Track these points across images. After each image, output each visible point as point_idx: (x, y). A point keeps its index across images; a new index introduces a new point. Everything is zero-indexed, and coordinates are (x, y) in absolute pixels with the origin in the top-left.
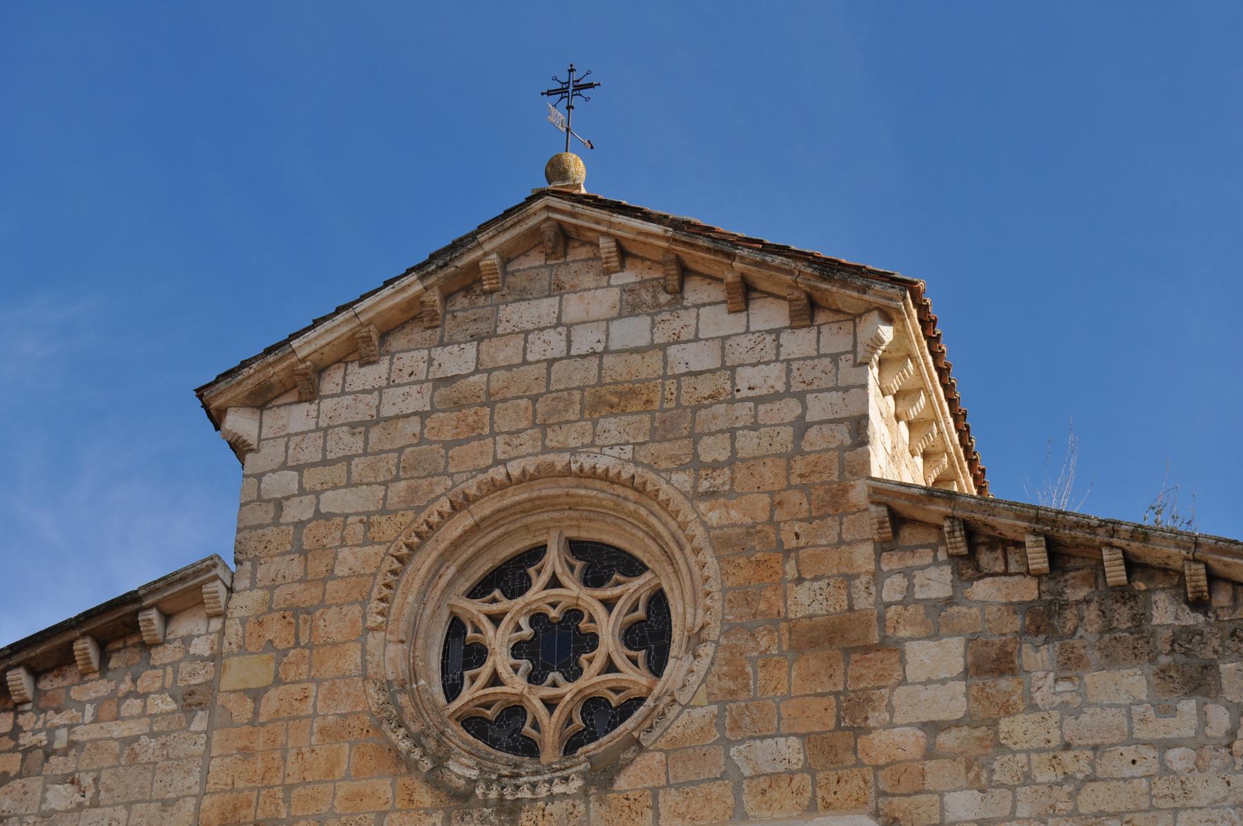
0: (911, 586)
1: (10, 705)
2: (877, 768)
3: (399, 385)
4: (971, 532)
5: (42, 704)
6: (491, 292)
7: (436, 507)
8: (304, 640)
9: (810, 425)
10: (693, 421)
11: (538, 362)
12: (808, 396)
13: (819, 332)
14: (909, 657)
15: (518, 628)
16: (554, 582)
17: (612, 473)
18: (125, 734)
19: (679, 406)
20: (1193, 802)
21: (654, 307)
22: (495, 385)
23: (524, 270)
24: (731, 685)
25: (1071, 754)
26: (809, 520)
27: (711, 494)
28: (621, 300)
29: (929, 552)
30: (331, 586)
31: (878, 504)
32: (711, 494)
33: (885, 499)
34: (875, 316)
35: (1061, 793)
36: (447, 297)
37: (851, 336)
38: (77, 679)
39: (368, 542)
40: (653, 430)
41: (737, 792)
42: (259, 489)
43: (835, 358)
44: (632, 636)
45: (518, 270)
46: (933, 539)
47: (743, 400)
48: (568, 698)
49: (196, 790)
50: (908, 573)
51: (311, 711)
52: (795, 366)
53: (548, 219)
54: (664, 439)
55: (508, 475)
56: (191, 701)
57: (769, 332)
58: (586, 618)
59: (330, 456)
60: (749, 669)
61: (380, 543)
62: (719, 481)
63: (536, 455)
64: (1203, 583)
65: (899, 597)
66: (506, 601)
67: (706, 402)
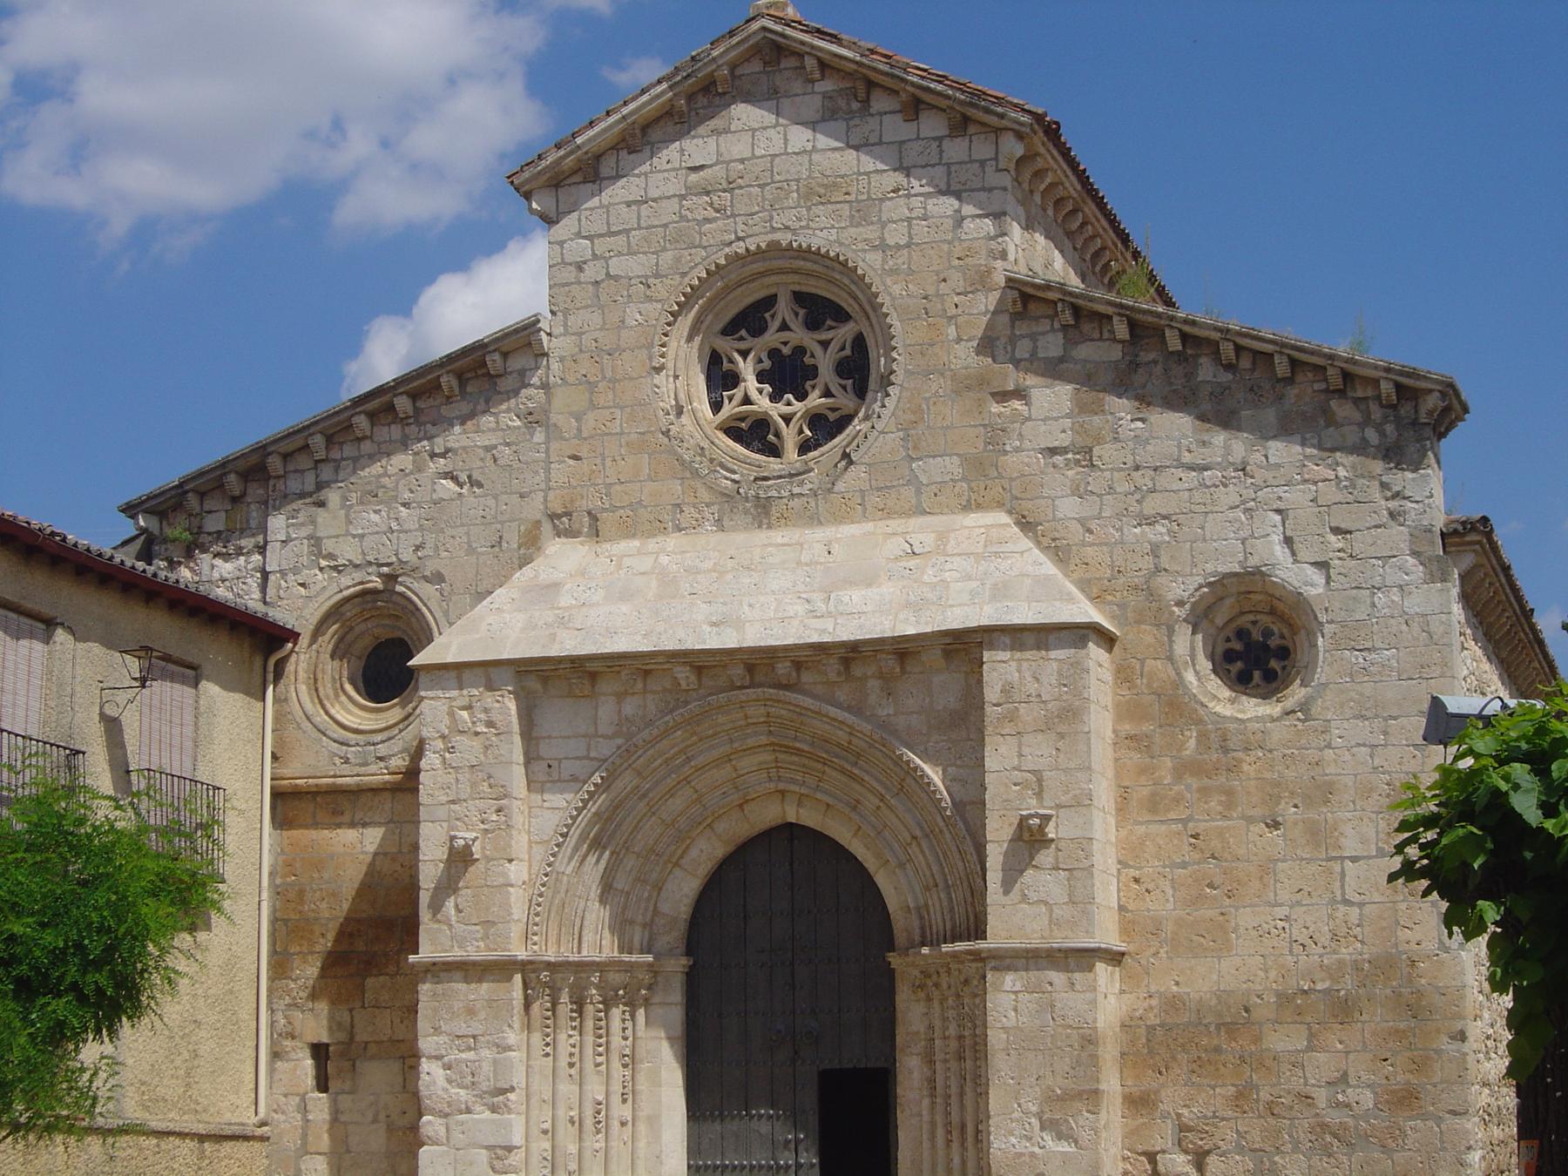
0: (1035, 348)
1: (398, 420)
2: (1012, 479)
3: (660, 171)
4: (1076, 311)
5: (423, 419)
6: (724, 94)
7: (695, 273)
8: (609, 374)
9: (963, 219)
10: (880, 211)
11: (763, 157)
12: (963, 194)
13: (971, 141)
14: (1034, 399)
15: (760, 361)
16: (784, 327)
17: (823, 251)
18: (487, 443)
19: (869, 198)
20: (1216, 509)
21: (849, 113)
22: (733, 175)
23: (748, 74)
24: (913, 418)
25: (1140, 473)
26: (965, 294)
27: (894, 272)
28: (823, 106)
29: (1048, 321)
30: (624, 333)
31: (1012, 288)
32: (894, 272)
33: (1017, 286)
34: (1010, 135)
35: (1132, 500)
36: (691, 98)
37: (994, 146)
38: (444, 400)
39: (649, 299)
40: (851, 217)
41: (919, 492)
42: (562, 254)
43: (982, 163)
44: (843, 369)
45: (743, 75)
46: (1051, 312)
47: (915, 195)
48: (799, 415)
49: (543, 486)
50: (1033, 337)
51: (618, 430)
52: (953, 168)
53: (765, 37)
54: (859, 225)
55: (747, 249)
56: (532, 419)
57: (934, 139)
58: (808, 354)
59: (614, 229)
60: (924, 406)
61: (657, 301)
62: (900, 261)
63: (766, 233)
64: (1232, 354)
65: (1027, 356)
66: (750, 339)
67: (889, 196)
